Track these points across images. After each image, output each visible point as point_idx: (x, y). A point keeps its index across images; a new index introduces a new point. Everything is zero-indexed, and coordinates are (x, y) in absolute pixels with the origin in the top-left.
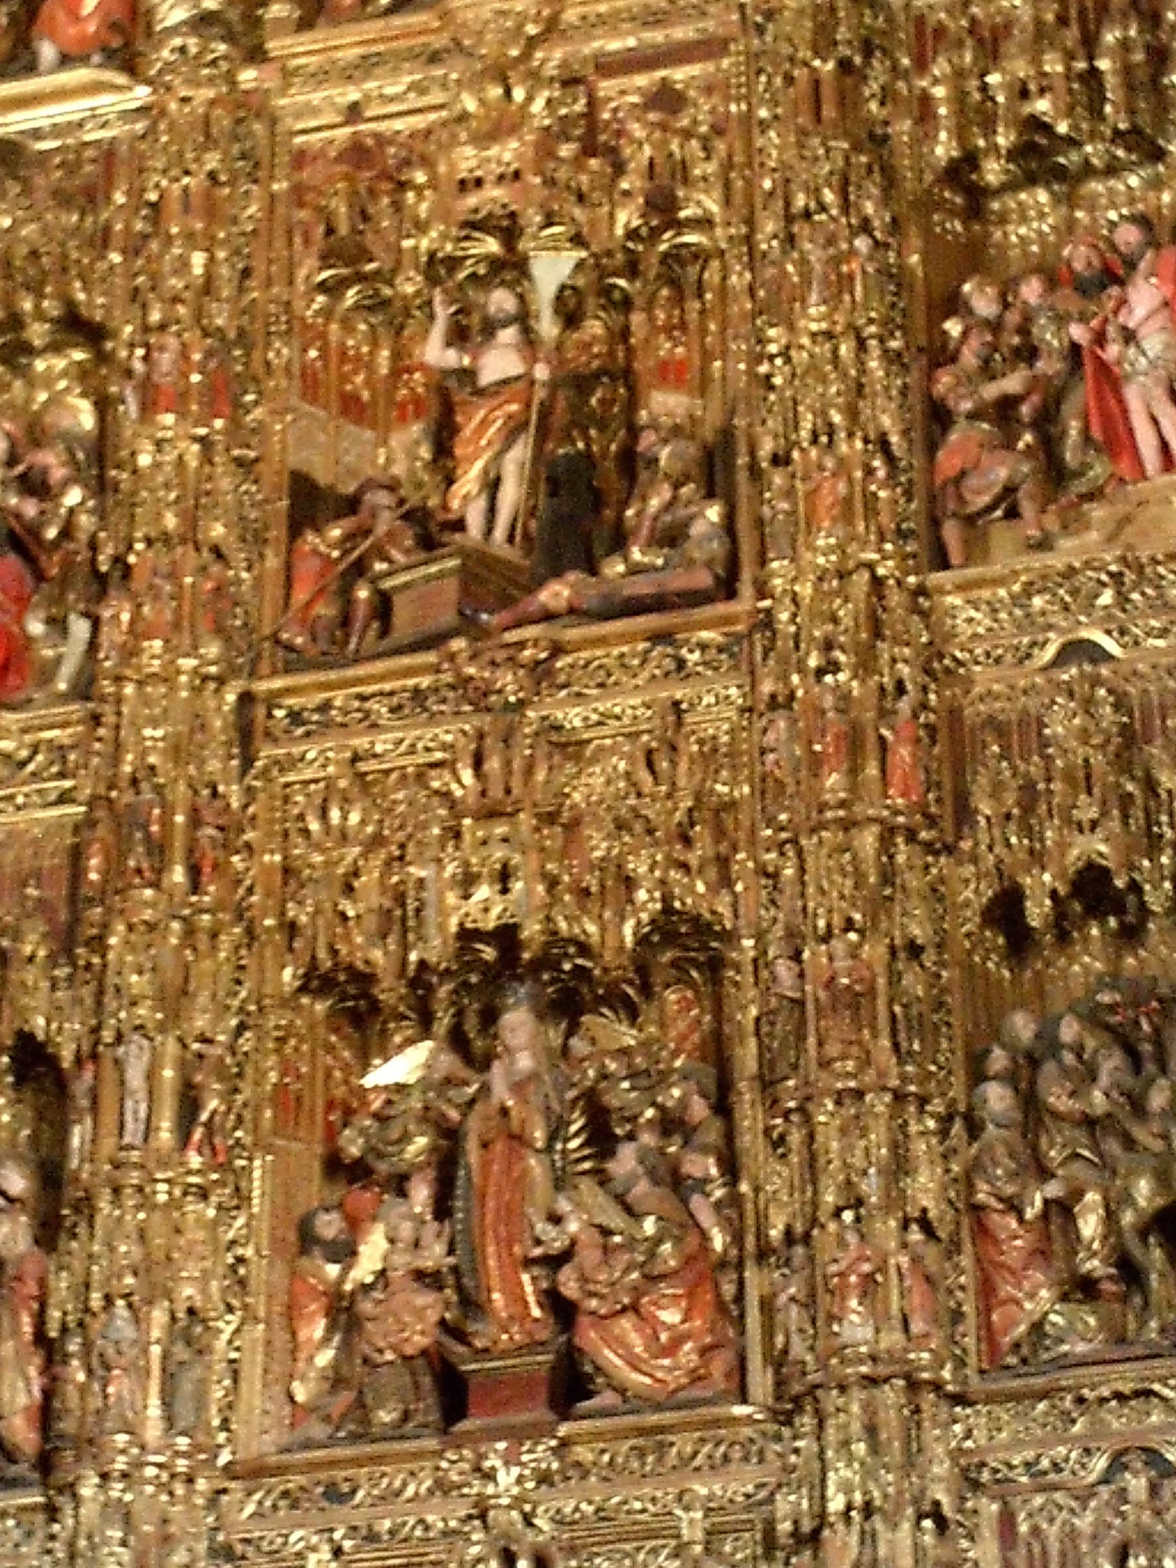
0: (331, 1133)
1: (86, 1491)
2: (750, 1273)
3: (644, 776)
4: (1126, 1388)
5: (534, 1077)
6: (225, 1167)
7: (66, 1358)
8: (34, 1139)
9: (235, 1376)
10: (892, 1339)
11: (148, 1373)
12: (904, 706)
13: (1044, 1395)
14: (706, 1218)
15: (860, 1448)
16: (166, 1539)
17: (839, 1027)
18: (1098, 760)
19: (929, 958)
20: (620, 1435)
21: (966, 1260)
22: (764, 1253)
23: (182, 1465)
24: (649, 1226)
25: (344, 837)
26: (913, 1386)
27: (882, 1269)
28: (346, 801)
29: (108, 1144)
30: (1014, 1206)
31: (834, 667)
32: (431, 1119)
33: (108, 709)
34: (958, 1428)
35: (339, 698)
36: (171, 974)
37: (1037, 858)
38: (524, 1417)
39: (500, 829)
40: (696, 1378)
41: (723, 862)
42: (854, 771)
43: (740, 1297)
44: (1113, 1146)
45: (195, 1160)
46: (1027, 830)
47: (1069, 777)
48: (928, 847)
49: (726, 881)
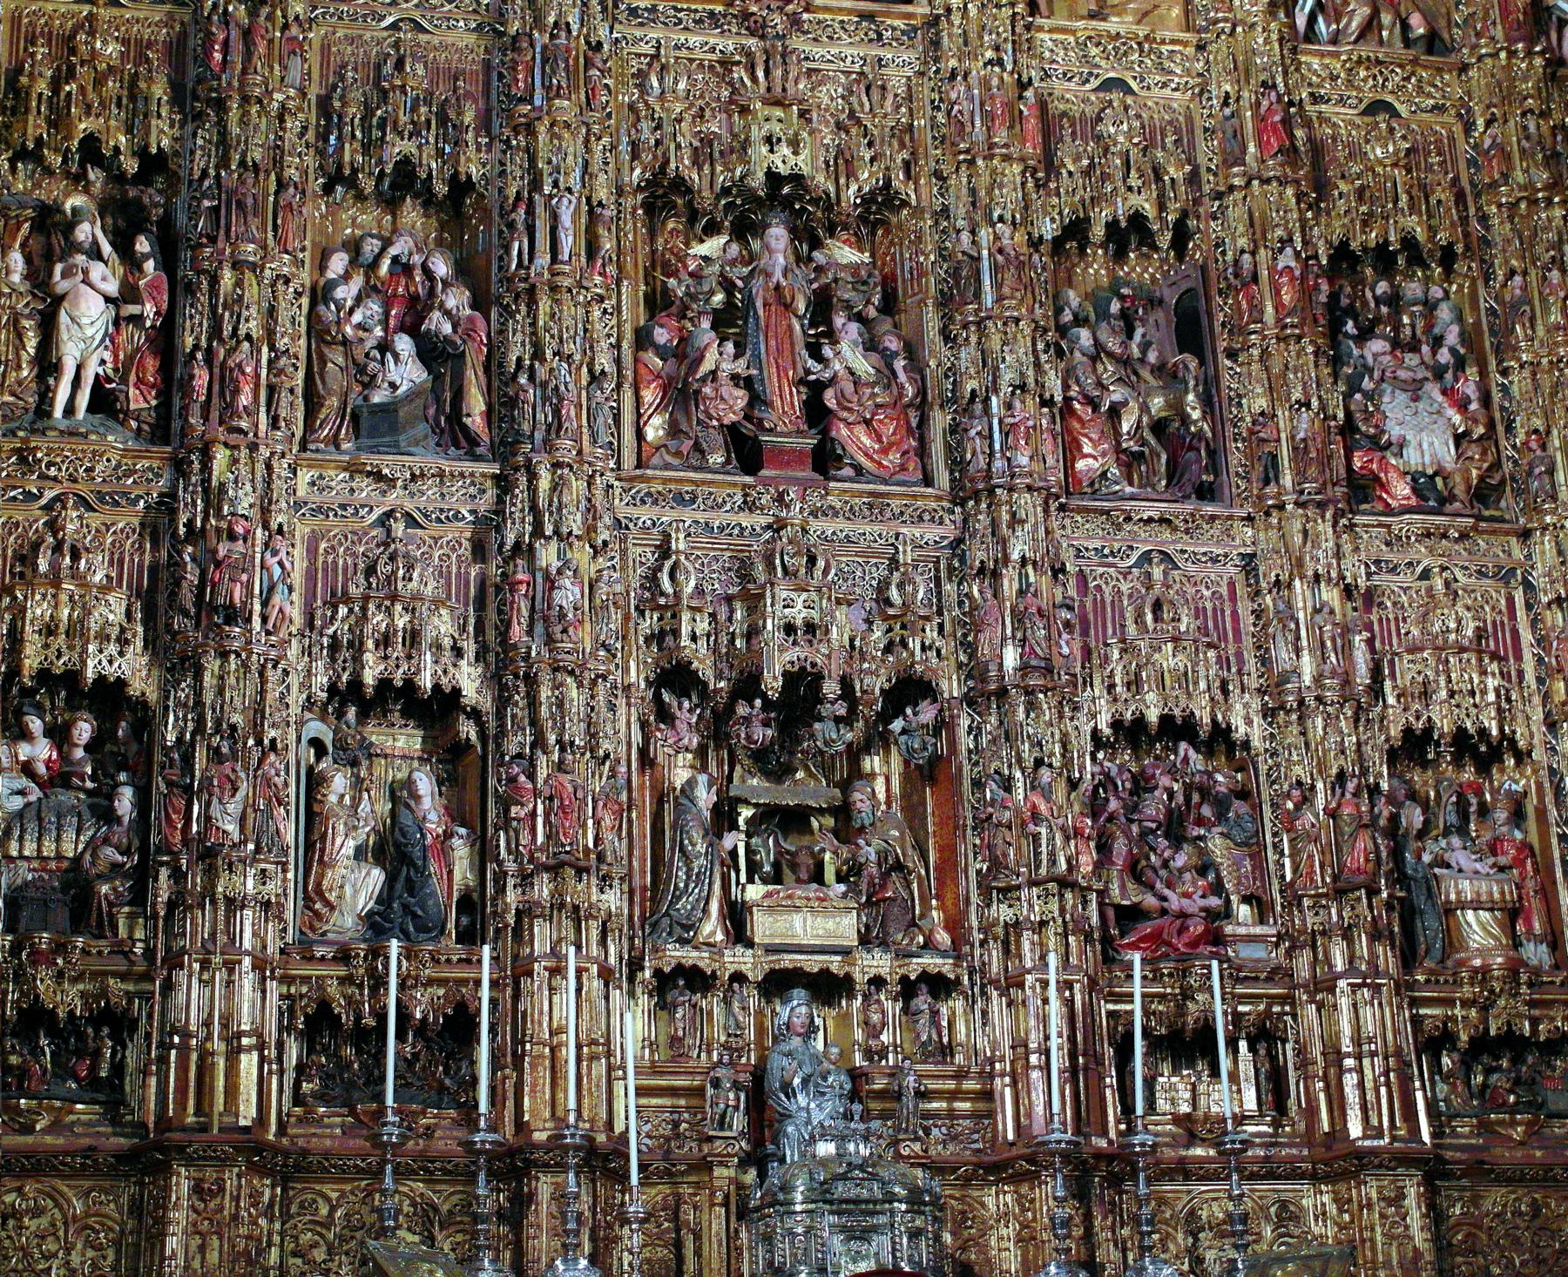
20: (861, 494)
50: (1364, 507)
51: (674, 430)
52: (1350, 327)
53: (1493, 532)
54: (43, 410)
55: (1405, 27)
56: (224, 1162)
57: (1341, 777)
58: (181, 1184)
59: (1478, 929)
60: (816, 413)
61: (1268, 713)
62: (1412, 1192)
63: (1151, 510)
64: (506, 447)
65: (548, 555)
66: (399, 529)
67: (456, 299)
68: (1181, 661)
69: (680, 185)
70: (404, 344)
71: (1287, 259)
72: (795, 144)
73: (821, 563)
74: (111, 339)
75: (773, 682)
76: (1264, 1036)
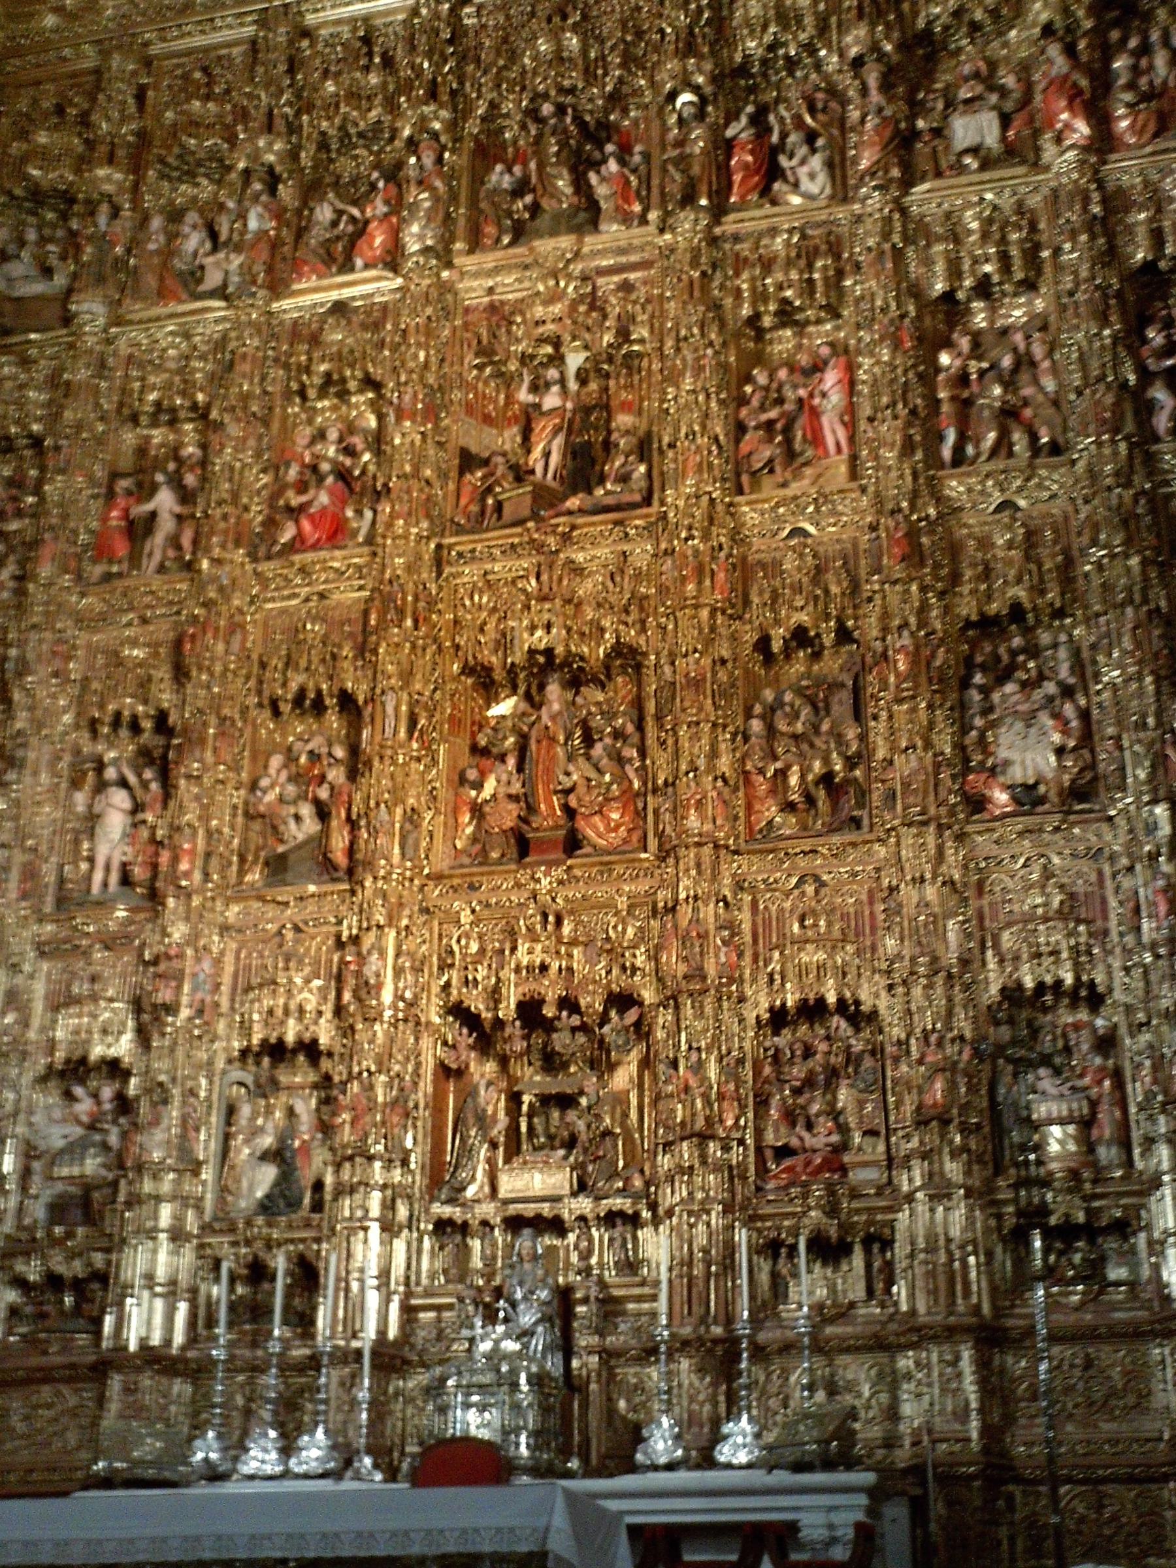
0: (473, 735)
1: (367, 884)
3: (610, 584)
5: (560, 713)
6: (429, 748)
8: (348, 735)
10: (708, 827)
12: (722, 554)
14: (631, 774)
15: (693, 872)
16: (401, 905)
17: (690, 695)
18: (805, 580)
19: (729, 665)
20: (593, 865)
21: (741, 794)
24: (607, 778)
25: (480, 607)
26: (716, 847)
28: (481, 592)
29: (378, 738)
30: (761, 771)
31: (692, 537)
32: (515, 730)
33: (380, 551)
35: (479, 547)
36: (406, 665)
37: (777, 622)
38: (552, 857)
39: (547, 606)
40: (625, 841)
41: (643, 622)
42: (700, 583)
44: (805, 747)
45: (415, 745)
46: (773, 610)
47: (792, 586)
48: (731, 617)
49: (644, 630)
51: (474, 839)
52: (978, 679)
53: (1085, 822)
54: (88, 891)
55: (1034, 437)
56: (139, 1370)
57: (926, 1034)
58: (115, 1383)
60: (570, 812)
61: (890, 987)
62: (966, 1354)
64: (350, 872)
65: (368, 940)
66: (289, 935)
67: (336, 775)
68: (821, 956)
69: (488, 670)
70: (306, 810)
71: (906, 640)
72: (548, 627)
73: (551, 918)
74: (129, 836)
75: (508, 1009)
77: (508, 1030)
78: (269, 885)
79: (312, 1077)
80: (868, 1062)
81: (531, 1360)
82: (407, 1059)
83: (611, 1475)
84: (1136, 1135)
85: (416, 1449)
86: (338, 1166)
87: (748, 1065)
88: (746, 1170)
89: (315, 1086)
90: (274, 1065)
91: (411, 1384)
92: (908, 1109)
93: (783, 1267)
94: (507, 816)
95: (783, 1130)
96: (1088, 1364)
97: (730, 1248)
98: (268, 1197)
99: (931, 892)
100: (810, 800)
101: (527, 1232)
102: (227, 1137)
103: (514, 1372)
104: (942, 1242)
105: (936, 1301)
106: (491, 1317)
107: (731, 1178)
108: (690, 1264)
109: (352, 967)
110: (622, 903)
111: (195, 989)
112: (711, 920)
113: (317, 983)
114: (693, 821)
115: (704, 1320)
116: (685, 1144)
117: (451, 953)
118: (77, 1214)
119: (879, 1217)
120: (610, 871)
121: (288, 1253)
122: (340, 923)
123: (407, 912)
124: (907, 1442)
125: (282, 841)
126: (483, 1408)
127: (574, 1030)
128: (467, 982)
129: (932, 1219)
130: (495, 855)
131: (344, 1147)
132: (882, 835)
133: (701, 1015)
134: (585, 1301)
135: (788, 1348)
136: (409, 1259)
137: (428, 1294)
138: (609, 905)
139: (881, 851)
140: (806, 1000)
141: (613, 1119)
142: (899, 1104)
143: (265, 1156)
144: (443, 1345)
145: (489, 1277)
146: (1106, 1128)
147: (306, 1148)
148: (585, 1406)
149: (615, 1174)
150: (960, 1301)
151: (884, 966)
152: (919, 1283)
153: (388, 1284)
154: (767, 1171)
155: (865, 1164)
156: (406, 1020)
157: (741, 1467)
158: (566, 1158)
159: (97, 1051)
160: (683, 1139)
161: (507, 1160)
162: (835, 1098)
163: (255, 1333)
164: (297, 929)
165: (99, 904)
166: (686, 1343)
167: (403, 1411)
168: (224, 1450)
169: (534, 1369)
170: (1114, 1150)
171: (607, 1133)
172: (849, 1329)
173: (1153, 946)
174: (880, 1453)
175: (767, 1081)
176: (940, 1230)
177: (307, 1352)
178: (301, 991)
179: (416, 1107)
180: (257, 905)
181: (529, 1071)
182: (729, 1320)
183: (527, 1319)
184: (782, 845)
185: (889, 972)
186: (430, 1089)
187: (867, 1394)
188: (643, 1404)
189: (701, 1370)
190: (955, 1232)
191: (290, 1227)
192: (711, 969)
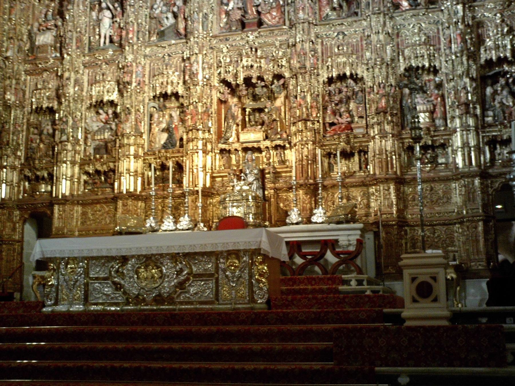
1: (192, 39)
2: (286, 8)
4: (340, 23)
7: (188, 21)
9: (212, 23)
10: (306, 16)
11: (199, 22)
13: (328, 24)
15: (301, 32)
16: (203, 46)
20: (267, 31)
21: (317, 5)
22: (288, 4)
23: (205, 36)
26: (309, 23)
27: (305, 6)
34: (315, 29)
38: (253, 28)
40: (278, 22)
43: (284, 11)
50: (397, 11)
51: (227, 23)
53: (434, 12)
54: (100, 45)
56: (127, 199)
57: (379, 84)
58: (120, 203)
59: (423, 118)
60: (259, 13)
61: (368, 69)
62: (392, 187)
63: (339, 22)
64: (186, 36)
65: (193, 59)
66: (167, 57)
68: (344, 59)
70: (170, 15)
73: (254, 50)
75: (240, 80)
76: (363, 152)
77: (241, 88)
78: (159, 41)
79: (177, 104)
80: (360, 94)
81: (253, 192)
82: (208, 98)
83: (279, 227)
84: (448, 116)
85: (217, 221)
86: (187, 133)
87: (320, 96)
88: (320, 130)
89: (178, 107)
90: (164, 101)
91: (214, 201)
92: (373, 109)
93: (332, 161)
94: (237, 15)
95: (332, 117)
96: (432, 189)
97: (315, 156)
98: (165, 143)
99: (381, 37)
100: (341, 6)
101: (250, 152)
102: (151, 124)
103: (247, 196)
104: (384, 152)
105: (382, 170)
106: (239, 179)
107: (315, 133)
108: (302, 161)
109: (188, 68)
110: (277, 44)
111: (136, 77)
112: (308, 48)
113: (177, 73)
114: (301, 15)
115: (307, 178)
116: (300, 123)
117: (221, 62)
118: (104, 151)
119: (363, 144)
120: (273, 33)
121: (173, 161)
122: (183, 53)
123: (205, 49)
124: (373, 215)
125: (162, 26)
126: (238, 207)
127: (263, 87)
128: (226, 72)
129: (381, 144)
130: (234, 28)
131: (189, 126)
132: (365, 18)
133: (304, 80)
134: (269, 173)
135: (334, 186)
136: (212, 162)
137: (219, 172)
138: (273, 44)
139: (365, 23)
140: (339, 74)
141: (276, 115)
142: (370, 108)
143: (163, 131)
144: (224, 188)
145: (238, 167)
146: (439, 113)
147: (176, 127)
148: (270, 205)
149: (277, 133)
150: (390, 170)
151: (366, 62)
152: (377, 165)
153: (206, 170)
154: (327, 130)
155: (359, 127)
156: (207, 85)
157: (320, 223)
158: (261, 128)
159: (106, 98)
160: (299, 121)
161: (242, 130)
162: (349, 106)
163: (164, 186)
164: (169, 56)
165: (103, 49)
166: (301, 185)
167: (212, 209)
168: (156, 222)
169: (253, 194)
170: (441, 121)
171: (275, 120)
172: (354, 180)
173: (456, 53)
174: (364, 218)
175: (327, 102)
176: (383, 148)
177: (181, 192)
178: (172, 76)
179: (212, 113)
180: (155, 48)
181: (248, 101)
182: (315, 178)
183: (251, 179)
184: (331, 22)
185: (367, 64)
186: (216, 107)
187: (360, 200)
188: (288, 205)
189: (306, 194)
190: (389, 148)
191: (173, 152)
192: (308, 65)
